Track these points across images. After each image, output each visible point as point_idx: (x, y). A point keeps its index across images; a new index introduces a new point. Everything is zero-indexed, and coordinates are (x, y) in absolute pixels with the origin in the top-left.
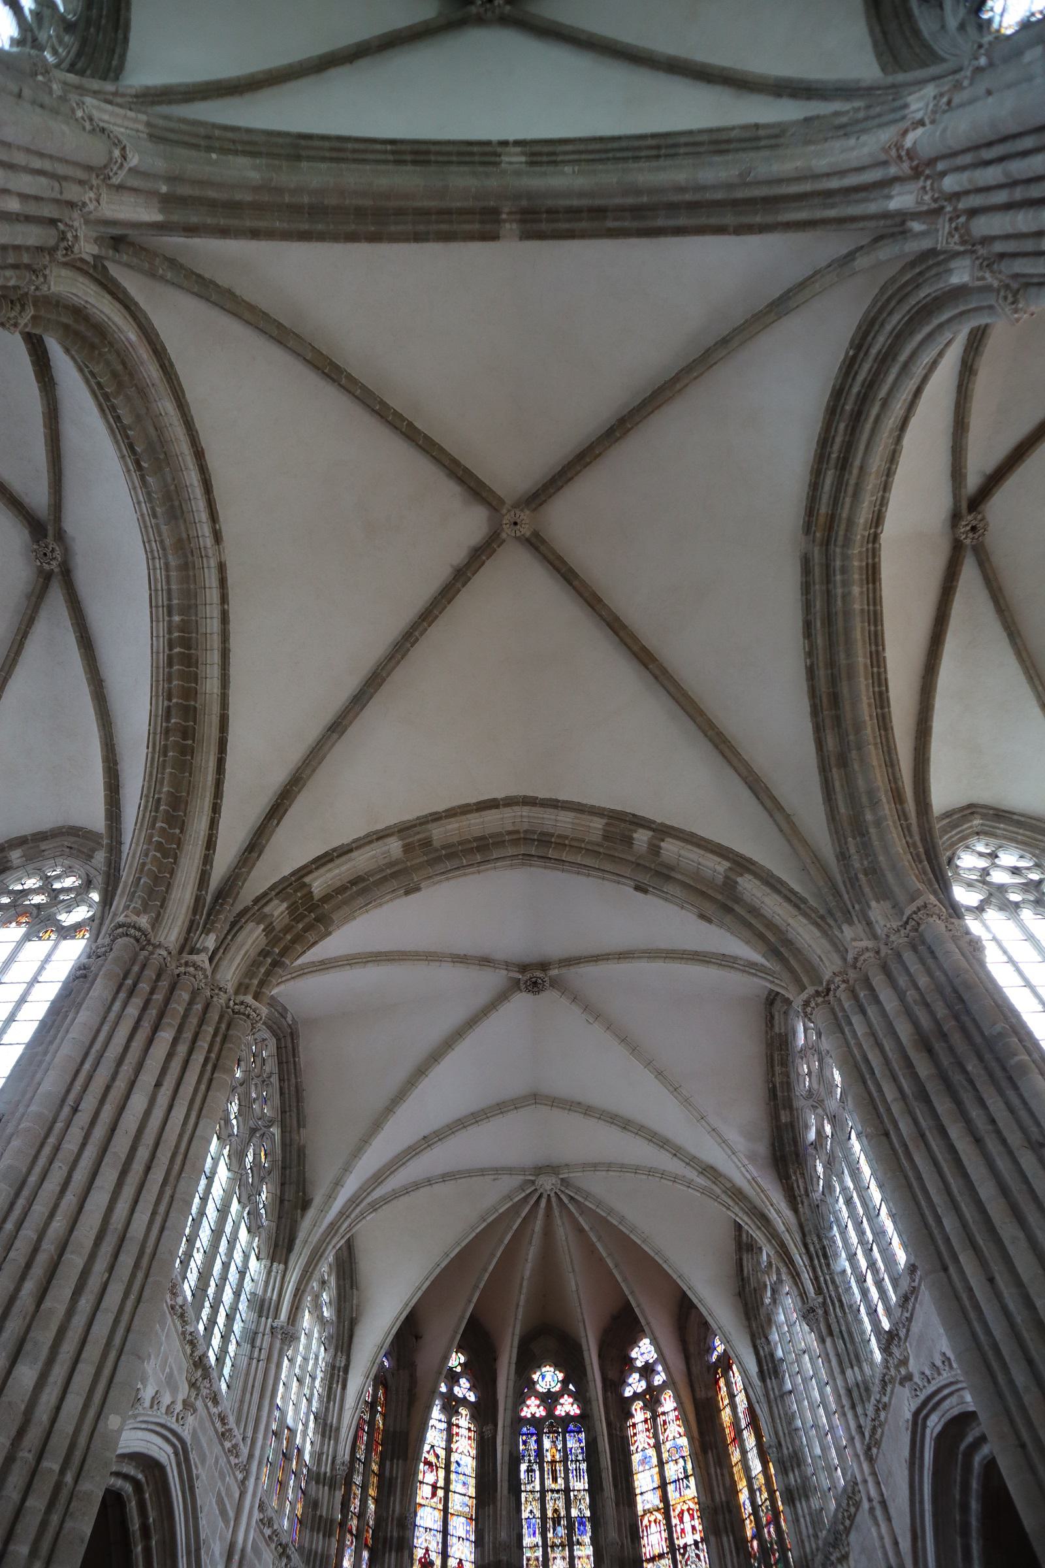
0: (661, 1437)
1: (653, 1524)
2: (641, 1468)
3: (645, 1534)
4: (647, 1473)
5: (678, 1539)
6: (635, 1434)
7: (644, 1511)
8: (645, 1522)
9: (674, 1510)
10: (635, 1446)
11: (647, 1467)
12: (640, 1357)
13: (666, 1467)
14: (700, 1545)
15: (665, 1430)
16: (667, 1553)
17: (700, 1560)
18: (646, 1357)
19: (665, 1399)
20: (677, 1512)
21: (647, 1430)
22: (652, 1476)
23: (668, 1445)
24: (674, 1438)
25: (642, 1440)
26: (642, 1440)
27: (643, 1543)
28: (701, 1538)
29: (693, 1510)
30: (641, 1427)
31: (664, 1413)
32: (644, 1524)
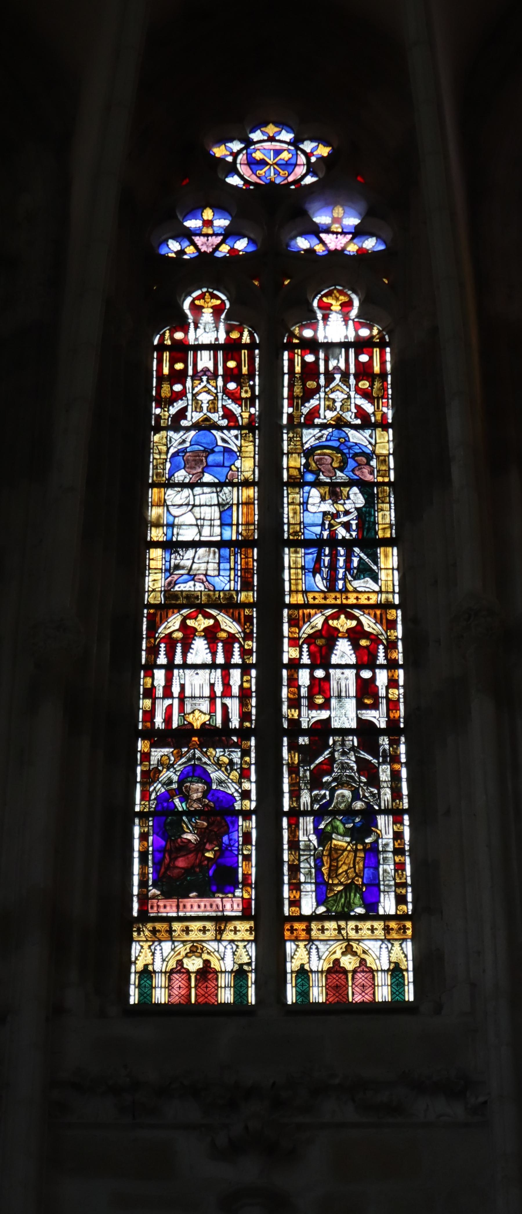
0: (287, 410)
1: (200, 646)
2: (181, 476)
3: (162, 660)
4: (205, 496)
5: (295, 704)
6: (179, 377)
7: (169, 593)
8: (173, 623)
9: (294, 622)
10: (173, 410)
11: (207, 478)
12: (244, 170)
13: (290, 496)
14: (384, 742)
15: (308, 395)
16: (243, 733)
17: (374, 781)
18: (268, 174)
19: (326, 308)
20: (307, 630)
21: (230, 375)
22: (224, 508)
23: (310, 437)
24: (340, 424)
25: (204, 398)
26: (204, 398)
27: (145, 682)
28: (392, 723)
29: (368, 636)
30: (205, 360)
31: (312, 345)
32: (162, 631)
